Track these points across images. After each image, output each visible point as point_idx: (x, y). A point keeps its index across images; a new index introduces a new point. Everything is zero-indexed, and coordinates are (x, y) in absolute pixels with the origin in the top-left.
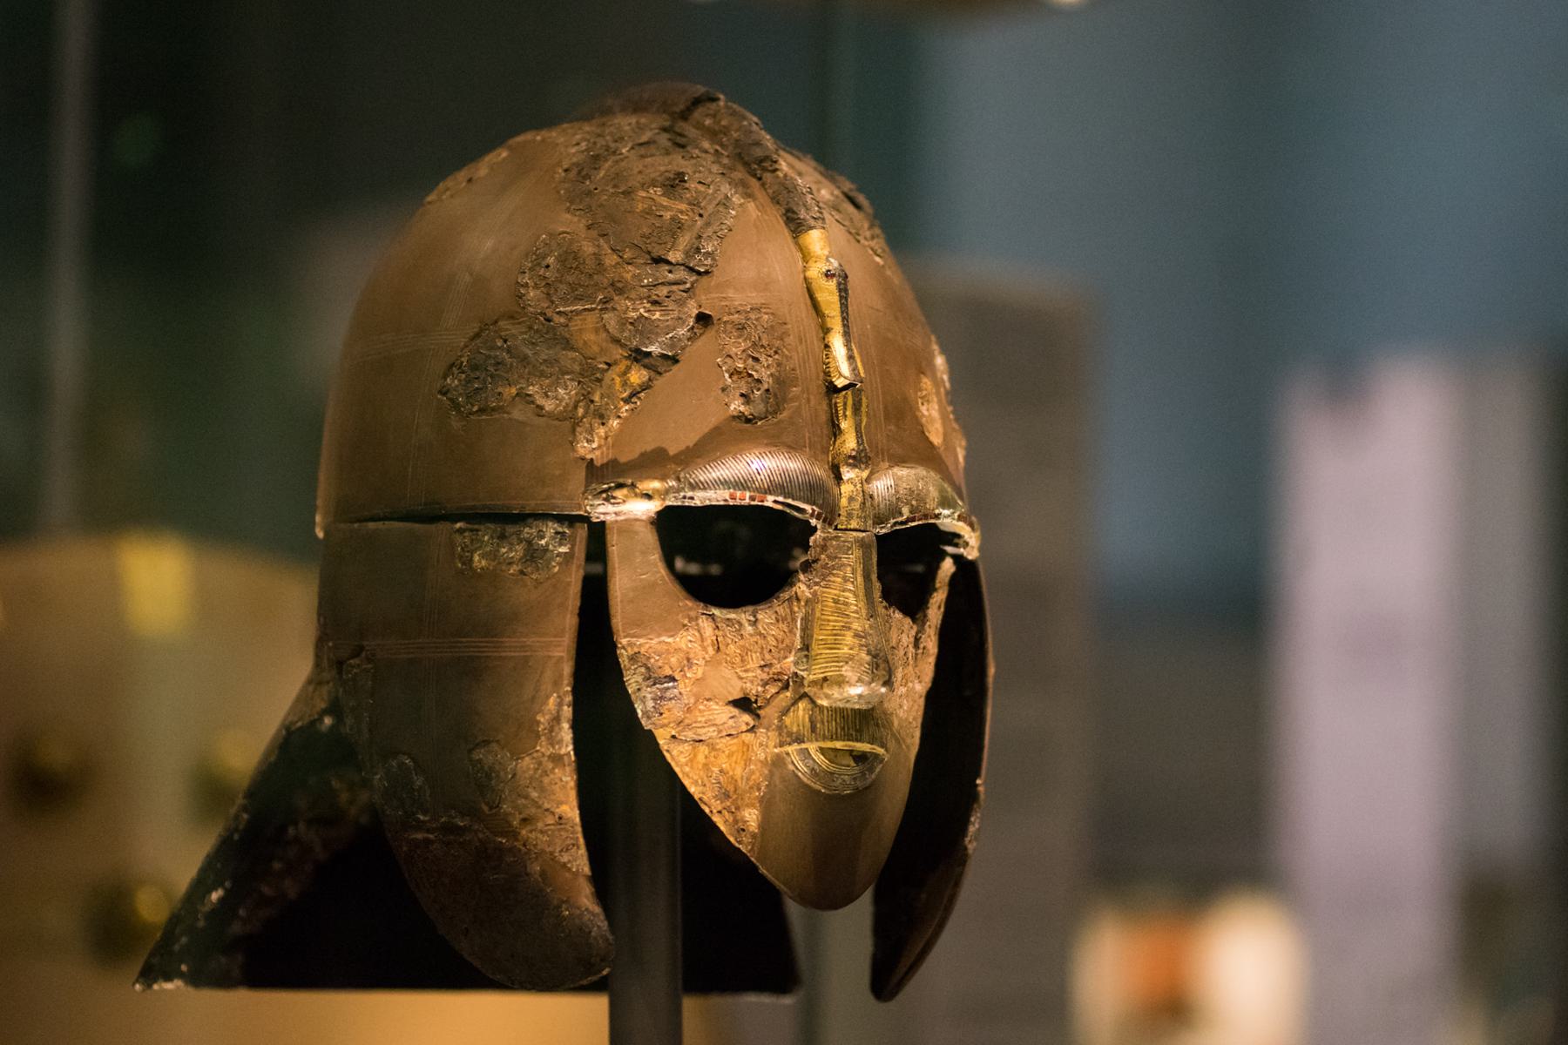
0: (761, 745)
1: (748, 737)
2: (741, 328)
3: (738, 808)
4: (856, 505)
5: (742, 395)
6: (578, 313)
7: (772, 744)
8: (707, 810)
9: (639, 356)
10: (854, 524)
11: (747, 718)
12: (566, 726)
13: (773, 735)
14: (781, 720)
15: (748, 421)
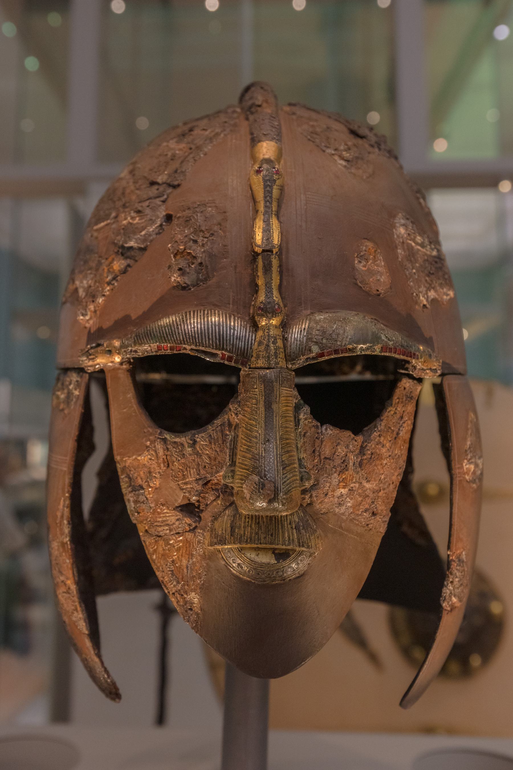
0: (199, 542)
1: (189, 536)
2: (188, 220)
4: (263, 348)
7: (207, 542)
8: (166, 591)
9: (124, 252)
10: (261, 363)
11: (188, 520)
13: (207, 534)
14: (213, 521)
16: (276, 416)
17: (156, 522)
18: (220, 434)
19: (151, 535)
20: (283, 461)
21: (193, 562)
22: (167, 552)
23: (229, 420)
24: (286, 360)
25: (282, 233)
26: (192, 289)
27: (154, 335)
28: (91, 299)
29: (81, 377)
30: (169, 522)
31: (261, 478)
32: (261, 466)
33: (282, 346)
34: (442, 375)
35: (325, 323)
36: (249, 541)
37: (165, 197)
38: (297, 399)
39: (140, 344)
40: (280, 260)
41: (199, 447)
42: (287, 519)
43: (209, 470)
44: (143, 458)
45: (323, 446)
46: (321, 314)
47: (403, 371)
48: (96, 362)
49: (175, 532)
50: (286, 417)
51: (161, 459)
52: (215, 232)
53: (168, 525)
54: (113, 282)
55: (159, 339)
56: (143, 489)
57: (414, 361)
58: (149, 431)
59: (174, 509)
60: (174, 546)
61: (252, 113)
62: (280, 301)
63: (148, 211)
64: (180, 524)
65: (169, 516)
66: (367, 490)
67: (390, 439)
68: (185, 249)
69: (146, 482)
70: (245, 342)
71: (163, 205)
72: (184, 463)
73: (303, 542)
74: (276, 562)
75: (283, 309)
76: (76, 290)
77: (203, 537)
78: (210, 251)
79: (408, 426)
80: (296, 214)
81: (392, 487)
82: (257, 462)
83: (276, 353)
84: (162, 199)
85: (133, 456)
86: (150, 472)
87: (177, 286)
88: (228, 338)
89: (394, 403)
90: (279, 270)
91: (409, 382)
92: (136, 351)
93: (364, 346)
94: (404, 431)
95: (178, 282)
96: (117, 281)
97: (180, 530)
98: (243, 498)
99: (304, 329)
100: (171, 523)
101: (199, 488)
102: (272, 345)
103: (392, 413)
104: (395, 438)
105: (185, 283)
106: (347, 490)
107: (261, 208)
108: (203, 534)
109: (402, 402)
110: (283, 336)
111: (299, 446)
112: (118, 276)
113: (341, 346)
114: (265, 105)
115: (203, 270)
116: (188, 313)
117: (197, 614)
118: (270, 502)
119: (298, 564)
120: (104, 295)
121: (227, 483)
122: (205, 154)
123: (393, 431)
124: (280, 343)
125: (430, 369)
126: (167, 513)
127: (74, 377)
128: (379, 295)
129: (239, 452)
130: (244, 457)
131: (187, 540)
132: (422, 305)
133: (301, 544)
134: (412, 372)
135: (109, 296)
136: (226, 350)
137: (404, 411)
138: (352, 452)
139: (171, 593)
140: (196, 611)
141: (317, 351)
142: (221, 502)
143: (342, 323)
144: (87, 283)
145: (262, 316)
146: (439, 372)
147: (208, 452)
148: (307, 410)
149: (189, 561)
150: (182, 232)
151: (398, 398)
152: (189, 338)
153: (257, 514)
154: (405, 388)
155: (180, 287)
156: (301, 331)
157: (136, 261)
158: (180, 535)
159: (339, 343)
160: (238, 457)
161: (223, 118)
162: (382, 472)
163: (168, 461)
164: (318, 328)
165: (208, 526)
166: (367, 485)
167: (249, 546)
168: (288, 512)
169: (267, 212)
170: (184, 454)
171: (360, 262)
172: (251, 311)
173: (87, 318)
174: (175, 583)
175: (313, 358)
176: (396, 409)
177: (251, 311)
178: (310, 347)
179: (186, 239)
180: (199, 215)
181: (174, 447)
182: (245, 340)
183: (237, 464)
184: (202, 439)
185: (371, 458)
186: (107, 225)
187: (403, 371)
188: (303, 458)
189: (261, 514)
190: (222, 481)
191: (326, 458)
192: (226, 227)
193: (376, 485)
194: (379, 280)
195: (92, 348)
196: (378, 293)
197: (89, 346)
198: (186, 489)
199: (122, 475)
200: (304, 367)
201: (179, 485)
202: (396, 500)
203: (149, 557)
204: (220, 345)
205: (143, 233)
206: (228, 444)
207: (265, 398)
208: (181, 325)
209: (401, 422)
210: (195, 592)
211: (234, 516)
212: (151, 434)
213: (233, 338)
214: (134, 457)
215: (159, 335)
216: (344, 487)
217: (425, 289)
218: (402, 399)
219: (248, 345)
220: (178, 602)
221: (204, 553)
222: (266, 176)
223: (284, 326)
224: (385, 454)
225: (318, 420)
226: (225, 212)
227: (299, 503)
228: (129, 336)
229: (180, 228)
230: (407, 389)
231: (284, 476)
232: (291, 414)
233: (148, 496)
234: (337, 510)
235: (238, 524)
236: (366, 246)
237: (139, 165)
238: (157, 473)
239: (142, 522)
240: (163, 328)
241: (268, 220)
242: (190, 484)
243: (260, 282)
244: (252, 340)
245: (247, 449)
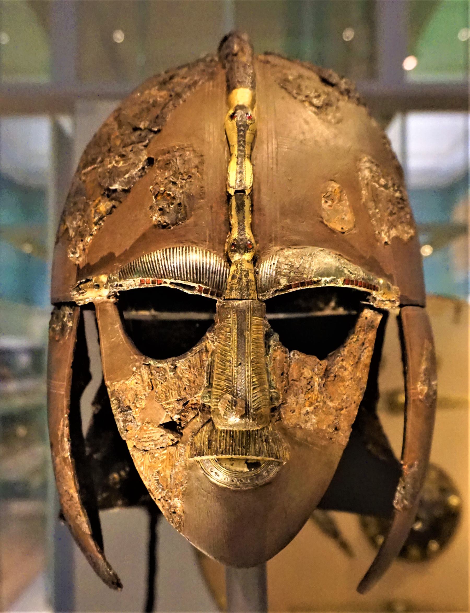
0: (181, 455)
1: (173, 449)
3: (170, 498)
4: (236, 281)
5: (160, 209)
6: (90, 172)
7: (187, 455)
8: (153, 498)
9: (109, 194)
10: (234, 295)
11: (171, 436)
12: (66, 439)
13: (188, 448)
15: (164, 227)
16: (248, 343)
17: (143, 438)
18: (198, 359)
19: (139, 450)
20: (253, 382)
21: (176, 472)
22: (153, 464)
23: (206, 347)
24: (257, 293)
25: (254, 174)
26: (172, 228)
27: (137, 270)
28: (80, 239)
29: (74, 310)
30: (154, 438)
32: (234, 386)
33: (253, 279)
34: (401, 306)
35: (293, 258)
36: (224, 452)
37: (147, 141)
38: (267, 328)
39: (125, 279)
40: (252, 200)
41: (180, 372)
42: (257, 433)
43: (189, 392)
44: (130, 382)
45: (291, 369)
46: (290, 249)
47: (365, 303)
48: (85, 296)
49: (159, 447)
50: (256, 343)
51: (146, 383)
52: (193, 174)
53: (153, 440)
54: (99, 223)
55: (141, 274)
56: (131, 409)
57: (374, 293)
58: (135, 358)
59: (158, 427)
60: (159, 459)
62: (252, 237)
63: (131, 155)
64: (163, 439)
65: (153, 433)
66: (330, 408)
67: (352, 364)
68: (165, 191)
69: (133, 403)
70: (220, 276)
71: (145, 149)
72: (166, 386)
73: (272, 453)
74: (248, 471)
75: (255, 245)
76: (67, 230)
77: (184, 450)
79: (369, 351)
80: (268, 157)
81: (353, 406)
82: (231, 382)
83: (247, 285)
84: (144, 143)
85: (121, 381)
86: (136, 395)
87: (158, 225)
88: (204, 272)
89: (356, 331)
90: (251, 209)
91: (370, 313)
92: (121, 285)
93: (328, 279)
94: (365, 356)
95: (159, 221)
96: (103, 221)
97: (164, 445)
98: (218, 415)
99: (274, 264)
100: (156, 439)
101: (180, 407)
102: (244, 278)
103: (354, 340)
104: (357, 363)
105: (165, 222)
106: (312, 408)
107: (235, 151)
108: (184, 448)
109: (364, 330)
110: (255, 271)
111: (269, 369)
112: (104, 217)
113: (307, 278)
114: (240, 54)
115: (182, 210)
116: (168, 250)
117: (180, 516)
118: (242, 417)
119: (268, 472)
120: (92, 235)
121: (206, 402)
122: (185, 101)
123: (355, 356)
124: (251, 277)
125: (389, 300)
126: (152, 430)
127: (68, 310)
128: (344, 233)
129: (215, 375)
130: (219, 379)
131: (170, 453)
132: (383, 242)
133: (271, 455)
134: (373, 303)
135: (96, 235)
136: (203, 283)
137: (365, 339)
138: (317, 375)
139: (157, 499)
140: (179, 514)
141: (285, 284)
142: (200, 420)
143: (309, 258)
144: (76, 224)
145: (235, 251)
146: (398, 304)
147: (187, 376)
148: (276, 337)
149: (172, 471)
150: (163, 175)
151: (360, 327)
153: (231, 429)
154: (366, 318)
155: (161, 226)
158: (163, 449)
159: (305, 276)
160: (215, 379)
161: (201, 66)
162: (344, 392)
163: (152, 385)
164: (287, 263)
165: (189, 441)
166: (331, 404)
167: (224, 456)
168: (258, 426)
169: (241, 156)
170: (166, 378)
171: (326, 202)
172: (226, 248)
173: (77, 255)
174: (160, 490)
175: (282, 290)
176: (358, 337)
177: (226, 248)
178: (279, 280)
179: (166, 181)
180: (178, 158)
181: (157, 372)
183: (214, 385)
184: (182, 363)
185: (334, 380)
186: (93, 169)
187: (365, 303)
188: (273, 380)
189: (235, 429)
190: (201, 401)
191: (293, 380)
192: (203, 170)
193: (339, 404)
194: (344, 219)
195: (81, 283)
197: (79, 282)
198: (168, 409)
199: (112, 398)
200: (273, 298)
201: (162, 405)
202: (358, 417)
203: (137, 468)
204: (197, 278)
205: (127, 176)
206: (206, 368)
207: (238, 327)
208: (161, 260)
209: (363, 348)
210: (178, 497)
211: (211, 431)
212: (136, 361)
214: (122, 381)
215: (142, 270)
216: (310, 406)
217: (387, 227)
218: (364, 327)
219: (223, 278)
220: (163, 506)
221: (185, 464)
222: (240, 121)
223: (255, 261)
224: (347, 377)
225: (286, 346)
226: (202, 156)
227: (269, 420)
228: (115, 271)
229: (160, 171)
230: (369, 318)
231: (254, 395)
232: (262, 341)
233: (135, 416)
234: (303, 426)
235: (214, 438)
236: (333, 187)
237: (124, 112)
238: (144, 396)
239: (130, 439)
240: (146, 264)
241: (242, 163)
242: (172, 404)
243: (234, 221)
245: (222, 372)
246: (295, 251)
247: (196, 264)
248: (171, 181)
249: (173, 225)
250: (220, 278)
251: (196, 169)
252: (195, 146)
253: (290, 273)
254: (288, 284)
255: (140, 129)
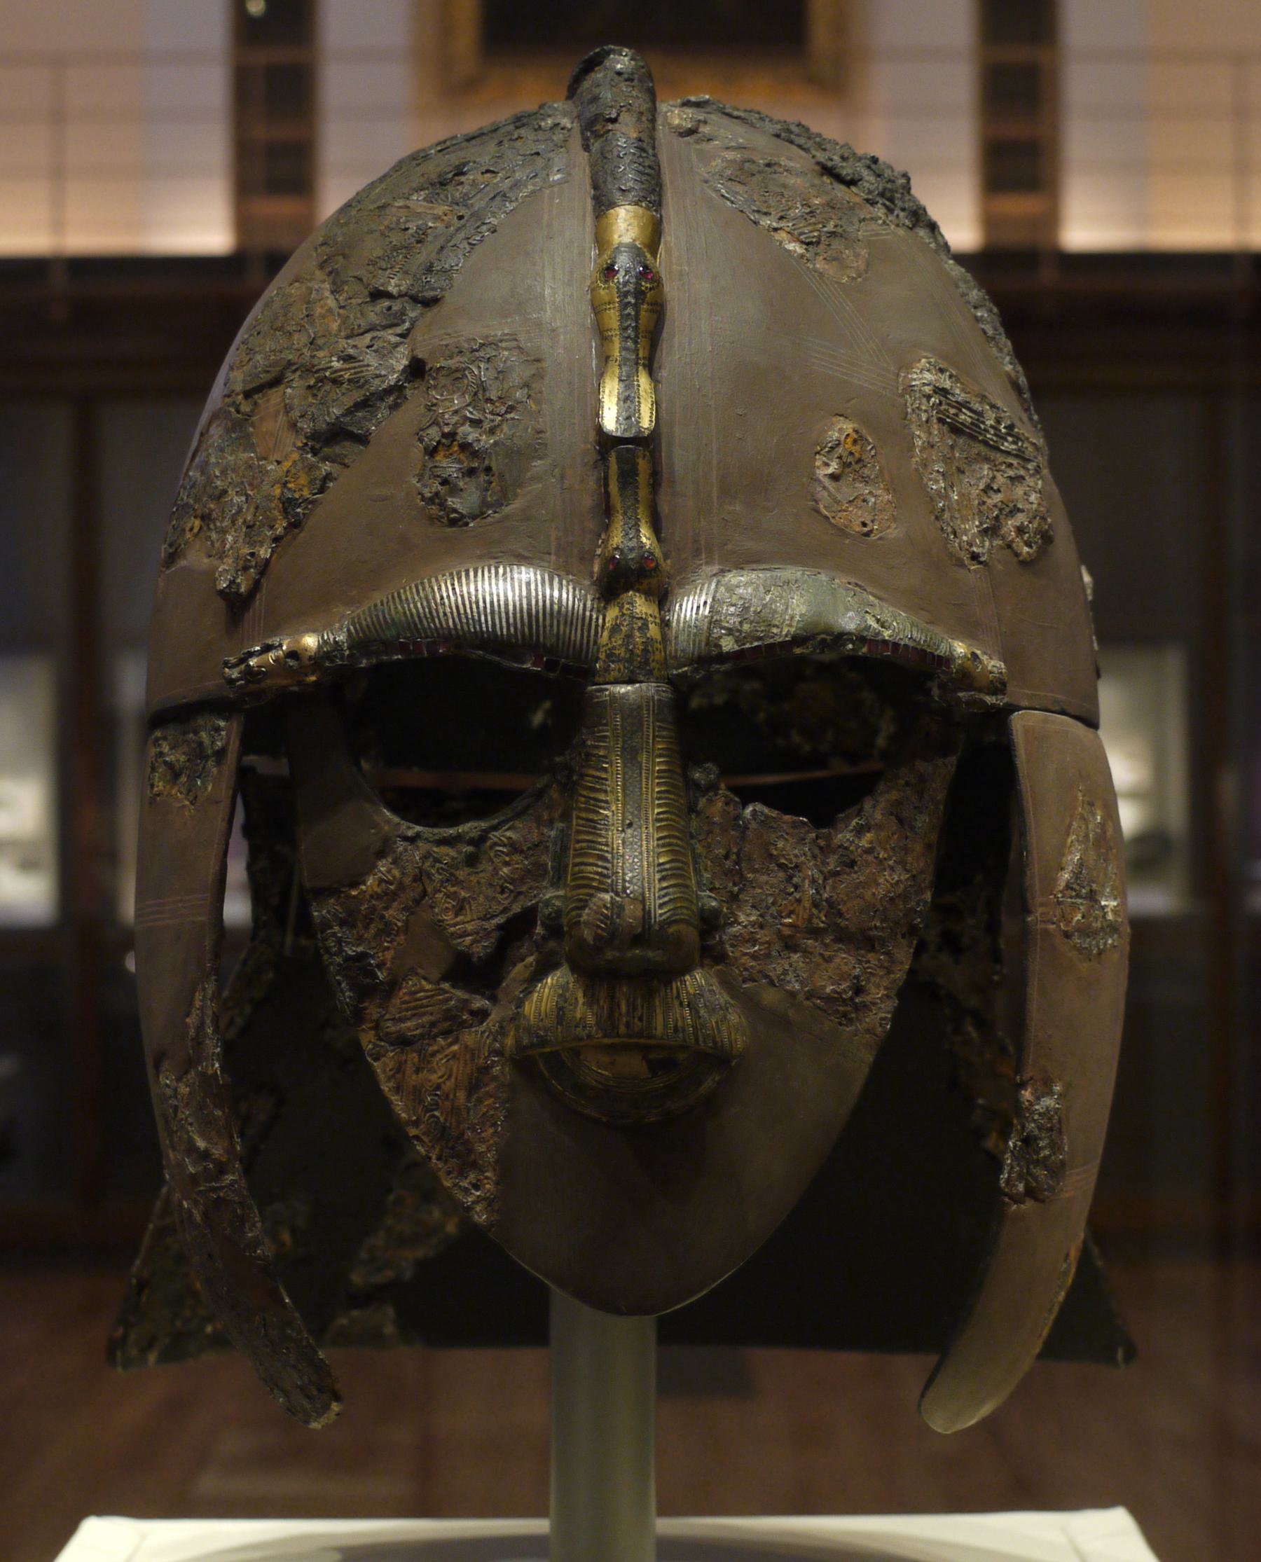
4: (618, 640)
25: (657, 404)
31: (617, 894)
33: (659, 638)
37: (407, 325)
61: (597, 136)
78: (508, 443)
83: (645, 651)
84: (399, 330)
88: (548, 622)
99: (705, 603)
107: (616, 350)
110: (662, 620)
124: (654, 631)
150: (448, 404)
152: (468, 623)
156: (698, 607)
157: (346, 466)
159: (775, 630)
164: (734, 602)
179: (456, 418)
182: (583, 625)
196: (865, 529)
213: (558, 622)
219: (589, 636)
226: (538, 360)
228: (337, 625)
231: (663, 893)
236: (841, 430)
244: (597, 626)
246: (753, 575)
247: (529, 604)
248: (466, 418)
249: (474, 518)
250: (582, 635)
251: (526, 390)
252: (522, 337)
253: (741, 623)
254: (737, 648)
255: (389, 296)
